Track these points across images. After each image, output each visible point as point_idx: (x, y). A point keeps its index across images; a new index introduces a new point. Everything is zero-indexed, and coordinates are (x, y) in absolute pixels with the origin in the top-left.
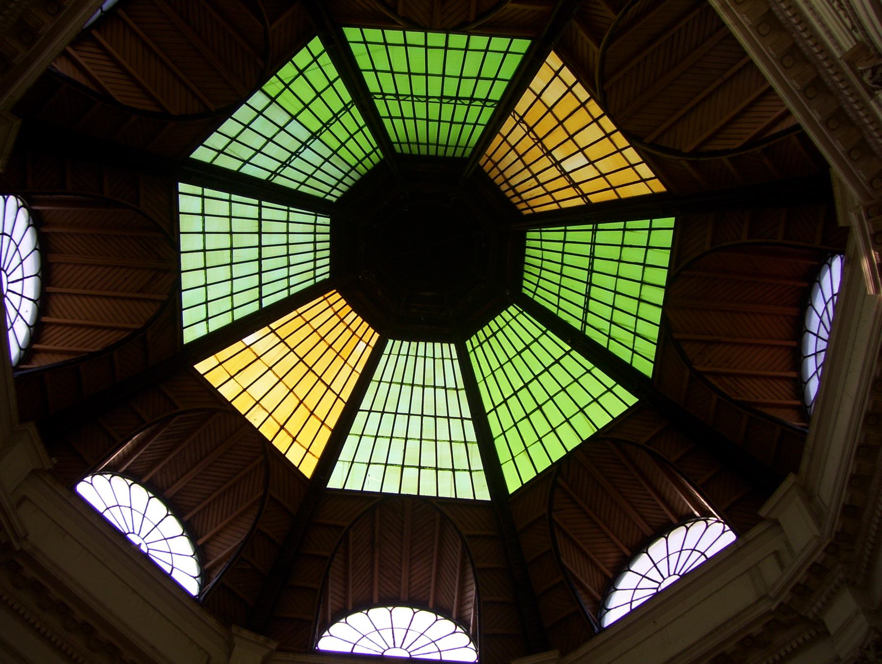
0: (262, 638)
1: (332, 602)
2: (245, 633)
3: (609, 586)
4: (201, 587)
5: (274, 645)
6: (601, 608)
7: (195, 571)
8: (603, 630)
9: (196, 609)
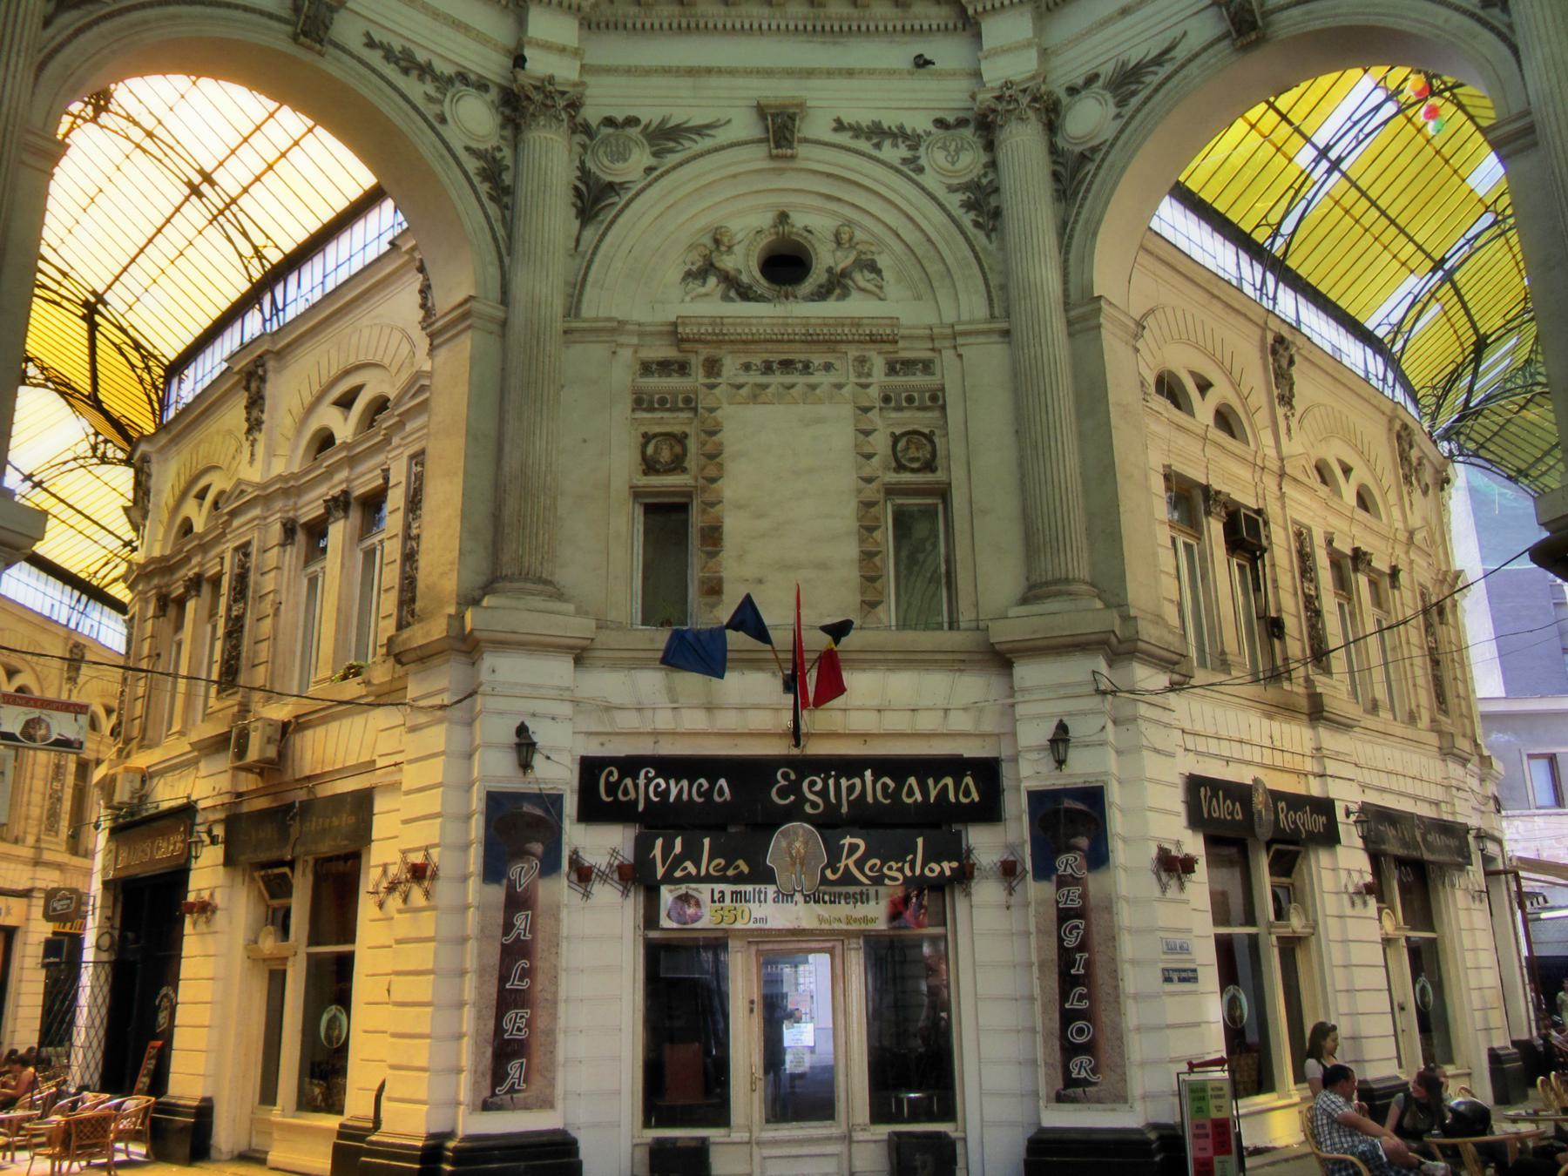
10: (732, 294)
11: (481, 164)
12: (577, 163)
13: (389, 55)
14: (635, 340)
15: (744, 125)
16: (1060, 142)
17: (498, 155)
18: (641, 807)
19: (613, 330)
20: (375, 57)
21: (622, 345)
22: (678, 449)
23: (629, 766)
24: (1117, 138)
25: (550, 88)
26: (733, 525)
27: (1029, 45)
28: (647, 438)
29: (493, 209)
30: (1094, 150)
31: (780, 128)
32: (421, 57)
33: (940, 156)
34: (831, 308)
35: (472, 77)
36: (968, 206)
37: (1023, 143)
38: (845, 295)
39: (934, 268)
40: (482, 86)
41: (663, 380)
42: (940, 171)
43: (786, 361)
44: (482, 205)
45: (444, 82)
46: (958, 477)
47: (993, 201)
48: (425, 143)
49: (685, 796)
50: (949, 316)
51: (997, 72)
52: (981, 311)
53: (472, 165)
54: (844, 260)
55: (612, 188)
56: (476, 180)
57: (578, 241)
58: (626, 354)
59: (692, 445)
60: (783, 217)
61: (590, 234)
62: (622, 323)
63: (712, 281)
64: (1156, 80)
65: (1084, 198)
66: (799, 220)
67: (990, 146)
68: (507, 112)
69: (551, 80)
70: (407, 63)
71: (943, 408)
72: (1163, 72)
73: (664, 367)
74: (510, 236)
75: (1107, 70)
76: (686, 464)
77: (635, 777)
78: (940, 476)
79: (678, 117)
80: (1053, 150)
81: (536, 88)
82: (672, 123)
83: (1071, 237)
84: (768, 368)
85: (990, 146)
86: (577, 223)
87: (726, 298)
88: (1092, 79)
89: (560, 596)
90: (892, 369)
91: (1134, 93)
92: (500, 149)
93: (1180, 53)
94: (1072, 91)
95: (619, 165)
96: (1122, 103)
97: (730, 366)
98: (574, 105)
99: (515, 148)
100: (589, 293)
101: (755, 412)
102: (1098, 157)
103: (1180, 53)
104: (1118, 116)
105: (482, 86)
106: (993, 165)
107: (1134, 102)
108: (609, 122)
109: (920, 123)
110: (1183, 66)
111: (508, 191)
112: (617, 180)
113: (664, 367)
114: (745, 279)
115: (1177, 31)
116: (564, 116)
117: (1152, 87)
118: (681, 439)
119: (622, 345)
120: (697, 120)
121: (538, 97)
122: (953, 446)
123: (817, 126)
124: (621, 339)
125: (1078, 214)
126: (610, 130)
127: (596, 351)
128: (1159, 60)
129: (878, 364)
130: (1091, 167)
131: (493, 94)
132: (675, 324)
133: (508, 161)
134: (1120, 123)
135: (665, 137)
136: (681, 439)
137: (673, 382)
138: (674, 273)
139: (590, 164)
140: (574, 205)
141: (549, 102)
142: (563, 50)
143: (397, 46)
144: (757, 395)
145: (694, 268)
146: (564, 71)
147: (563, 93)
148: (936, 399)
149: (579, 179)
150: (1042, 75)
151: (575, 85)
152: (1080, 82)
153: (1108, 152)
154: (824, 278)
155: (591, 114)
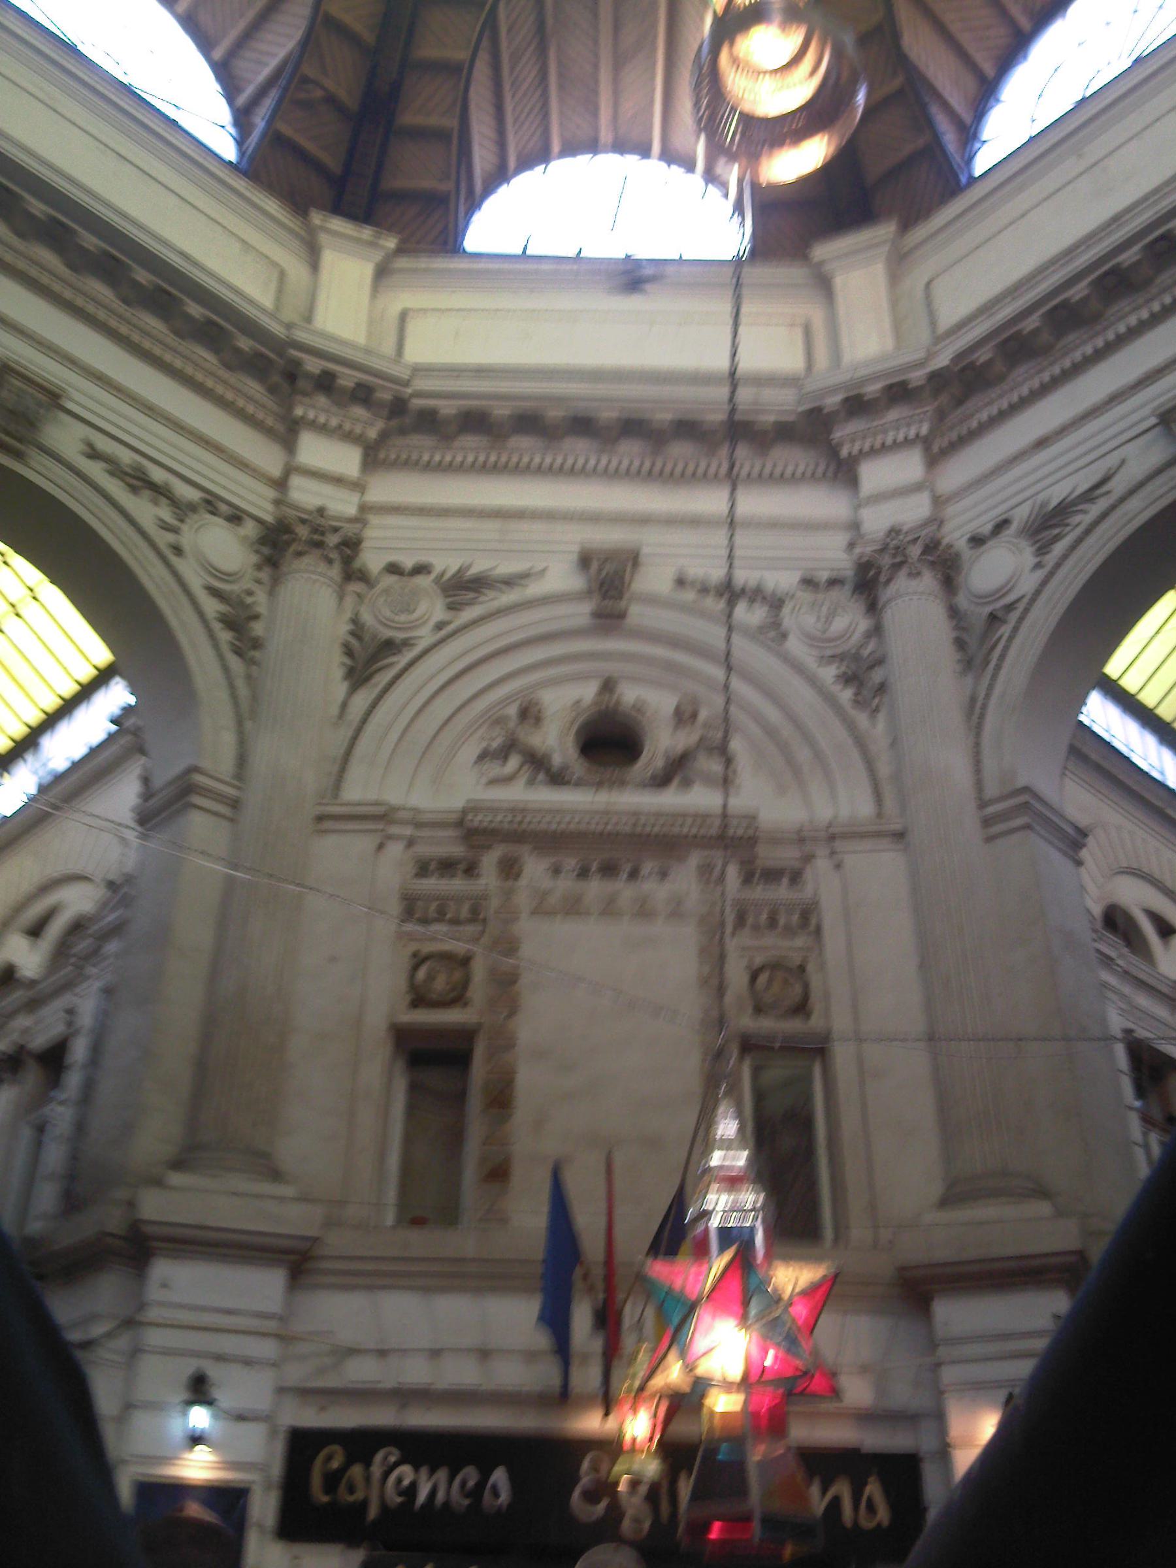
0: (367, 232)
1: (482, 158)
2: (338, 224)
3: (986, 91)
4: (240, 142)
5: (391, 243)
6: (969, 134)
7: (223, 112)
8: (973, 180)
9: (240, 184)
10: (541, 776)
11: (223, 608)
12: (348, 615)
13: (116, 469)
14: (408, 831)
15: (560, 576)
16: (962, 601)
17: (249, 600)
18: (373, 1512)
19: (381, 817)
20: (96, 470)
21: (390, 837)
22: (458, 975)
23: (362, 1444)
24: (1038, 593)
25: (322, 521)
26: (529, 1081)
27: (917, 488)
28: (419, 960)
29: (234, 662)
30: (1010, 607)
31: (609, 580)
32: (158, 475)
33: (809, 621)
34: (670, 799)
35: (223, 508)
36: (848, 679)
37: (915, 606)
38: (687, 783)
39: (803, 755)
40: (236, 517)
41: (444, 881)
42: (811, 639)
43: (612, 854)
44: (221, 657)
45: (183, 509)
46: (841, 1022)
47: (877, 676)
48: (152, 576)
49: (441, 1496)
50: (823, 812)
51: (877, 521)
52: (865, 808)
53: (212, 607)
54: (683, 740)
55: (389, 647)
56: (217, 626)
57: (344, 705)
58: (395, 850)
59: (479, 971)
60: (608, 686)
61: (361, 700)
62: (394, 809)
63: (514, 762)
64: (1087, 519)
65: (998, 667)
66: (629, 694)
67: (873, 608)
68: (266, 550)
69: (321, 511)
70: (139, 481)
71: (818, 930)
72: (1095, 509)
73: (447, 866)
74: (255, 698)
75: (1021, 515)
76: (469, 994)
77: (368, 1463)
78: (816, 1022)
79: (479, 566)
80: (954, 612)
81: (303, 521)
82: (473, 571)
83: (982, 716)
84: (583, 873)
85: (873, 608)
86: (342, 688)
87: (531, 782)
88: (1001, 525)
89: (276, 1175)
90: (748, 879)
91: (1056, 539)
92: (250, 593)
93: (1118, 486)
94: (977, 541)
95: (403, 618)
96: (1042, 550)
97: (535, 869)
98: (351, 546)
99: (271, 593)
100: (356, 771)
101: (563, 929)
102: (1014, 616)
103: (1118, 486)
104: (1038, 566)
105: (236, 517)
106: (877, 631)
107: (1059, 548)
108: (393, 569)
109: (783, 580)
110: (1122, 500)
111: (257, 644)
112: (399, 636)
113: (447, 866)
114: (557, 760)
115: (1112, 461)
116: (334, 555)
117: (1079, 531)
118: (465, 961)
119: (390, 837)
120: (506, 567)
121: (303, 532)
122: (831, 982)
123: (654, 579)
124: (394, 830)
125: (991, 687)
126: (392, 579)
127: (360, 844)
128: (1089, 496)
129: (733, 873)
130: (1005, 630)
131: (249, 529)
132: (464, 812)
133: (262, 609)
134: (1040, 574)
135: (463, 588)
136: (465, 961)
137: (457, 884)
138: (471, 750)
139: (367, 618)
140: (344, 664)
141: (316, 537)
142: (338, 481)
143: (126, 457)
144: (573, 908)
145: (495, 745)
146: (343, 504)
147: (336, 530)
148: (808, 918)
149: (353, 633)
150: (936, 520)
151: (351, 520)
152: (987, 529)
153: (1026, 610)
154: (660, 763)
155: (372, 560)
